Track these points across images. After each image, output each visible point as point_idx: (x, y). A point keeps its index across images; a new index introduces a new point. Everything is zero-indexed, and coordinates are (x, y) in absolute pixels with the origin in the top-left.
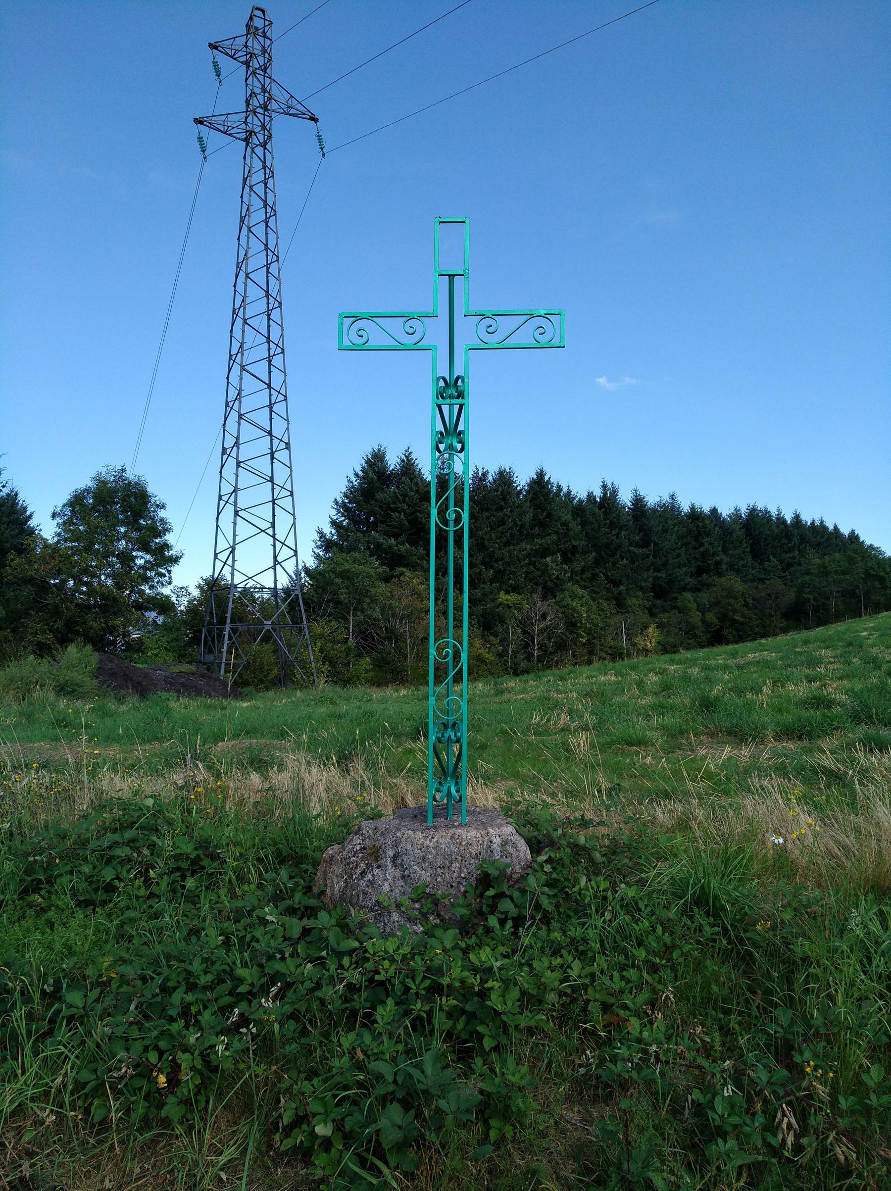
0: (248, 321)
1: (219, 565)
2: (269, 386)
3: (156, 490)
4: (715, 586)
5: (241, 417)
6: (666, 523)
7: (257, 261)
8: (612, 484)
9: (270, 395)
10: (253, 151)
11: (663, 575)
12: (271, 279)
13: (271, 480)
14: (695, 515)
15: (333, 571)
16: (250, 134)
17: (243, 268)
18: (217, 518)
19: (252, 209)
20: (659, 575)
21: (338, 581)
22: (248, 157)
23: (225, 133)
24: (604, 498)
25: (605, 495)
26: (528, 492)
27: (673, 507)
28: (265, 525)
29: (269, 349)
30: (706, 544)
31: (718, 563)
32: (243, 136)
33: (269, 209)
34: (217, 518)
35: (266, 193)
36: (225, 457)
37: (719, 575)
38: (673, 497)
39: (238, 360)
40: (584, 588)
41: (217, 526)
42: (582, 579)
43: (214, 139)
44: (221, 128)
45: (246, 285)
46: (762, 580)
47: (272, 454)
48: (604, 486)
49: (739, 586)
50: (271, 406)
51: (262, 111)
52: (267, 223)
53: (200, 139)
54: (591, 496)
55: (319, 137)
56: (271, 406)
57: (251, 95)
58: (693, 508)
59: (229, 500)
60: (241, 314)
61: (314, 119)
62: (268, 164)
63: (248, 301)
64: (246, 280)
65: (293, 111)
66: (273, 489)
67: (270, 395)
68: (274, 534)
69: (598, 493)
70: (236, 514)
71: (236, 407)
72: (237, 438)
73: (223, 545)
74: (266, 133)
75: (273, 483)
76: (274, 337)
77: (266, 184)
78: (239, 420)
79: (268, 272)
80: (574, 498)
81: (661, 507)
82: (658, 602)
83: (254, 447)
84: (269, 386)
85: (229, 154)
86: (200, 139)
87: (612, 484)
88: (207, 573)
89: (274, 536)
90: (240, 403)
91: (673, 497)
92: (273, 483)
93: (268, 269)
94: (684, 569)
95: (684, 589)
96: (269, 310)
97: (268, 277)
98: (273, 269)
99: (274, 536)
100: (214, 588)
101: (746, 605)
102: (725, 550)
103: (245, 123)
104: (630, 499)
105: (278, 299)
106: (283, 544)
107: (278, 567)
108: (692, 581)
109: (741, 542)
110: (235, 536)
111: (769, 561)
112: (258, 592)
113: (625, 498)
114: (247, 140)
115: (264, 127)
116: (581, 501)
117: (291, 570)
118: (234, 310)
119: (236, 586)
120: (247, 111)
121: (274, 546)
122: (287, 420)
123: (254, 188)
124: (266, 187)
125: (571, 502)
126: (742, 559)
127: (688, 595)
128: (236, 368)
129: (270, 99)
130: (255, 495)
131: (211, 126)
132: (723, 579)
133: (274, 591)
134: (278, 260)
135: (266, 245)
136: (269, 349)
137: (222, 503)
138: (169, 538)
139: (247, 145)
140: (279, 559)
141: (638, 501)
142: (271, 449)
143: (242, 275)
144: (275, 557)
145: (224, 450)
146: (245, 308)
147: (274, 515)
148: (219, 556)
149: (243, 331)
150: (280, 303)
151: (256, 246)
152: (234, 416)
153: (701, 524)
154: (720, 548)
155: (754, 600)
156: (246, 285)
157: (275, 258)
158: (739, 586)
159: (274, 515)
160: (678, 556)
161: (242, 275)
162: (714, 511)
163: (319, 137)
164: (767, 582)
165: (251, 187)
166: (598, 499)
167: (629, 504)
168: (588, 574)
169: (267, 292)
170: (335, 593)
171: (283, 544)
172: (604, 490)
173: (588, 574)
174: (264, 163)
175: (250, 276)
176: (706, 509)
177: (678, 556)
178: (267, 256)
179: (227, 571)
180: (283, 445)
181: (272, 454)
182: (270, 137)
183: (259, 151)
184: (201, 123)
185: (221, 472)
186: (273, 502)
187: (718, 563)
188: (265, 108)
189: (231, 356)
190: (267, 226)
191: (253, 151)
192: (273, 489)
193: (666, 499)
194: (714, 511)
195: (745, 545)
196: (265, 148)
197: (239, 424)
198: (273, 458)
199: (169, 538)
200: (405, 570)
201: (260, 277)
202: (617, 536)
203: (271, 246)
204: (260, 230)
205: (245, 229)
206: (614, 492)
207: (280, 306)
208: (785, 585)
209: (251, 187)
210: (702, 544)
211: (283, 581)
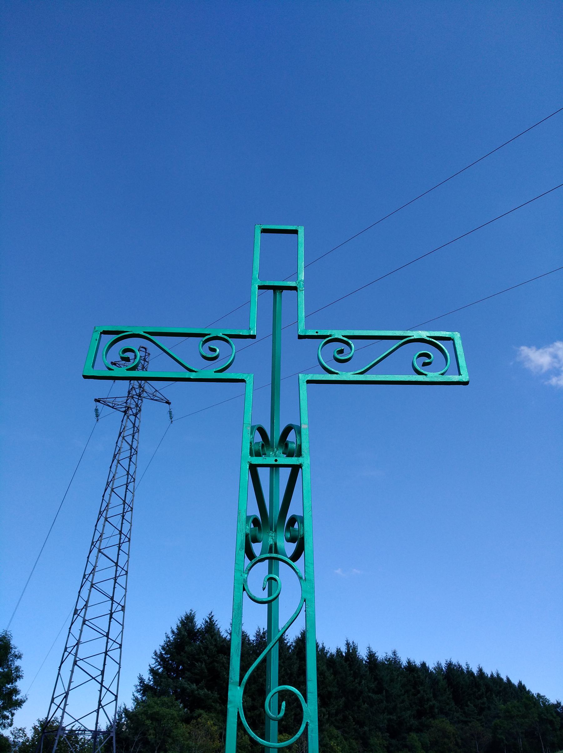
0: (108, 519)
1: (54, 707)
2: (117, 564)
3: (18, 643)
4: (433, 727)
5: (92, 586)
6: (392, 674)
7: (121, 480)
8: (353, 643)
9: (116, 571)
10: (128, 417)
11: (395, 718)
12: (128, 493)
13: (107, 636)
14: (411, 667)
15: (145, 713)
16: (128, 409)
17: (111, 485)
18: (60, 667)
19: (122, 450)
20: (391, 717)
21: (148, 722)
22: (124, 421)
23: (113, 407)
24: (348, 653)
25: (349, 650)
26: (295, 647)
27: (395, 661)
28: (96, 673)
29: (120, 539)
30: (422, 692)
31: (432, 707)
32: (124, 409)
33: (133, 450)
34: (60, 667)
35: (132, 441)
36: (76, 616)
37: (434, 717)
38: (394, 653)
39: (97, 545)
40: (338, 728)
41: (59, 674)
42: (336, 720)
43: (104, 410)
44: (111, 405)
45: (110, 496)
46: (466, 723)
47: (111, 614)
48: (348, 644)
49: (450, 728)
50: (115, 579)
51: (137, 397)
52: (130, 459)
53: (96, 410)
54: (339, 651)
55: (170, 413)
56: (115, 579)
57: (132, 389)
58: (409, 662)
59: (72, 653)
60: (104, 515)
61: (168, 403)
62: (137, 425)
63: (110, 506)
64: (111, 493)
65: (156, 398)
66: (107, 642)
67: (116, 571)
68: (102, 681)
69: (344, 649)
70: (75, 663)
71: (90, 579)
72: (87, 602)
73: (60, 690)
74: (138, 408)
75: (108, 638)
76: (125, 531)
77: (133, 436)
78: (91, 588)
79: (127, 488)
80: (327, 653)
81: (387, 661)
82: (394, 742)
83: (99, 608)
84: (117, 564)
85: (113, 419)
86: (96, 410)
87: (353, 643)
88: (43, 717)
89: (101, 684)
90: (94, 575)
91: (394, 653)
92: (108, 638)
93: (127, 486)
94: (409, 712)
95: (410, 730)
96: (124, 512)
97: (126, 492)
98: (131, 487)
99: (101, 684)
100: (48, 730)
101: (457, 744)
102: (435, 696)
103: (126, 403)
104: (366, 654)
105: (131, 506)
106: (108, 690)
107: (101, 710)
108: (414, 722)
109: (445, 690)
110: (70, 682)
111: (467, 706)
112: (81, 734)
113: (363, 653)
114: (125, 412)
115: (137, 405)
116: (332, 655)
117: (111, 715)
118: (100, 512)
119: (64, 729)
120: (128, 397)
121: (101, 691)
122: (126, 589)
123: (125, 438)
124: (133, 438)
125: (326, 656)
126: (448, 704)
127: (414, 735)
128: (95, 551)
129: (143, 391)
130: (92, 647)
131: (105, 403)
132: (437, 721)
133: (96, 733)
134: (134, 481)
135: (128, 472)
136: (120, 539)
137: (66, 654)
138: (19, 684)
139: (125, 415)
140: (103, 703)
141: (372, 656)
142: (111, 611)
143: (109, 490)
144: (100, 701)
145: (76, 610)
146: (107, 511)
147: (104, 664)
148: (55, 701)
149: (104, 526)
150: (132, 508)
151: (121, 472)
152: (88, 584)
153: (415, 674)
154: (431, 695)
155: (462, 739)
156: (110, 496)
157: (132, 480)
158: (450, 728)
159: (104, 664)
160: (403, 701)
161: (109, 490)
162: (424, 665)
163: (170, 413)
164: (470, 725)
165: (123, 438)
166: (344, 654)
167: (366, 658)
168: (340, 717)
169: (124, 501)
170: (144, 734)
171: (108, 690)
172: (348, 647)
173: (340, 717)
174: (134, 424)
175: (114, 490)
176: (418, 663)
177: (403, 701)
178: (128, 478)
179: (59, 713)
180: (120, 608)
181: (111, 614)
182: (140, 411)
183: (132, 418)
184: (99, 401)
185: (70, 628)
186: (106, 653)
187: (432, 707)
188: (139, 396)
189: (93, 542)
190: (130, 460)
191: (128, 417)
192: (107, 642)
193: (390, 655)
194: (424, 665)
195: (448, 693)
196: (136, 417)
197: (90, 591)
198: (111, 617)
199: (19, 684)
200: (201, 711)
201: (121, 491)
202: (360, 683)
203: (131, 472)
204: (125, 463)
205: (116, 461)
206: (355, 649)
207: (132, 510)
208: (483, 726)
209: (123, 438)
210: (419, 692)
211: (103, 726)
